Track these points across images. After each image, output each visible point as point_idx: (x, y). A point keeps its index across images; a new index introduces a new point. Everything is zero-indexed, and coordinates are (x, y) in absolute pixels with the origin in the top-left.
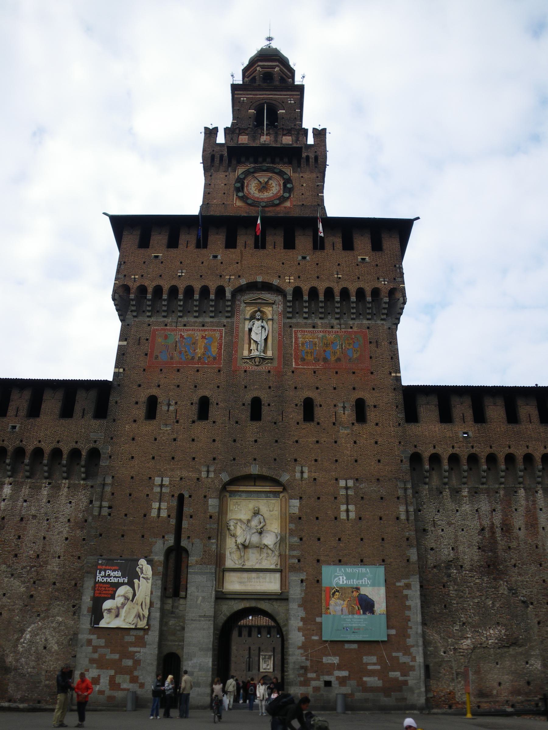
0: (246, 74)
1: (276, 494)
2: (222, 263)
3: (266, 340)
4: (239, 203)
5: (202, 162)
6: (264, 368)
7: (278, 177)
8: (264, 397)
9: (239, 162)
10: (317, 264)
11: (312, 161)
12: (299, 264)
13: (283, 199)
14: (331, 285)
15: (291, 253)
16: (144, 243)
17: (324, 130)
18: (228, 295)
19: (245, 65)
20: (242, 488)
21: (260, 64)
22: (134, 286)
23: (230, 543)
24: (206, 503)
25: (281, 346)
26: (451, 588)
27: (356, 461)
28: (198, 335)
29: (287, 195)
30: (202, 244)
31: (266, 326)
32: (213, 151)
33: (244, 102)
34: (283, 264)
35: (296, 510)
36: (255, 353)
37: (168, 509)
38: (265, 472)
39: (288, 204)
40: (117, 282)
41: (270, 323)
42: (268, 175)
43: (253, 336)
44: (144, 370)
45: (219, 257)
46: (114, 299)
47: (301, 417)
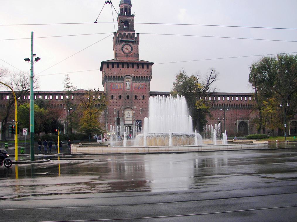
1: (131, 110)
4: (123, 53)
6: (129, 90)
8: (129, 95)
9: (122, 42)
11: (136, 42)
13: (131, 52)
15: (133, 69)
16: (108, 67)
18: (123, 78)
22: (107, 76)
23: (125, 117)
24: (122, 112)
25: (132, 87)
28: (118, 84)
29: (131, 51)
30: (118, 67)
36: (128, 88)
39: (132, 53)
43: (127, 85)
47: (135, 98)
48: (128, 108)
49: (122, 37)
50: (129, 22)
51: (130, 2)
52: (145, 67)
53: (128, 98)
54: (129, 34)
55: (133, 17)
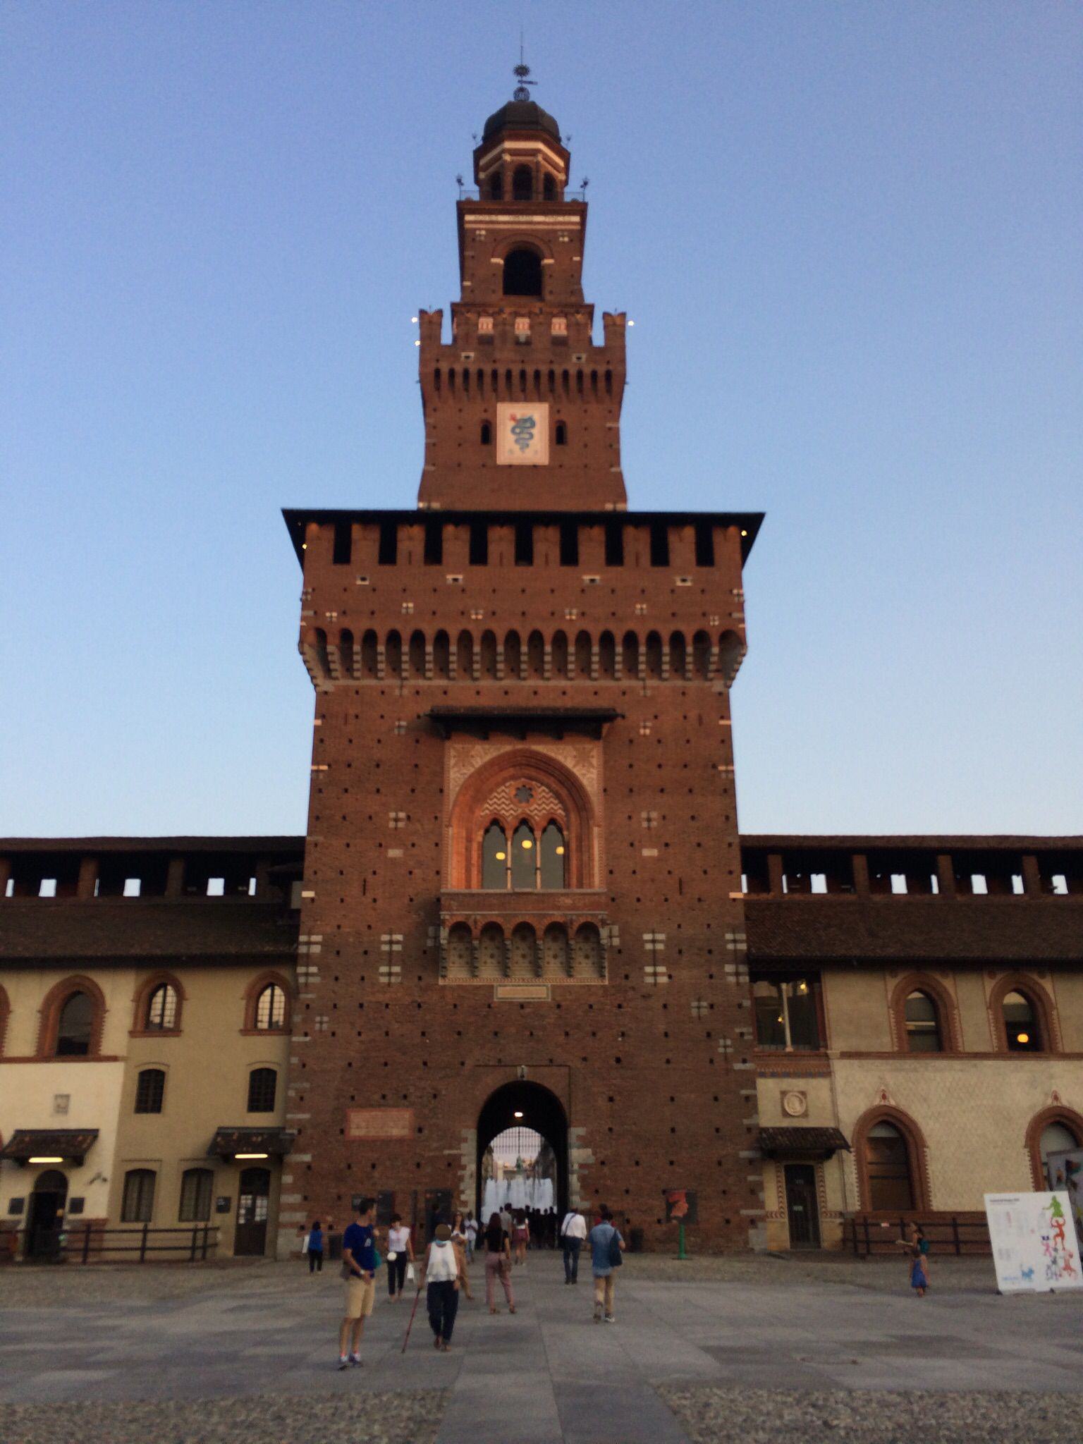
0: (482, 162)
5: (418, 379)
14: (631, 625)
16: (342, 554)
19: (480, 142)
21: (508, 145)
30: (434, 554)
33: (480, 241)
40: (304, 624)
45: (461, 582)
46: (302, 653)
50: (546, 252)
51: (559, 140)
55: (576, 219)
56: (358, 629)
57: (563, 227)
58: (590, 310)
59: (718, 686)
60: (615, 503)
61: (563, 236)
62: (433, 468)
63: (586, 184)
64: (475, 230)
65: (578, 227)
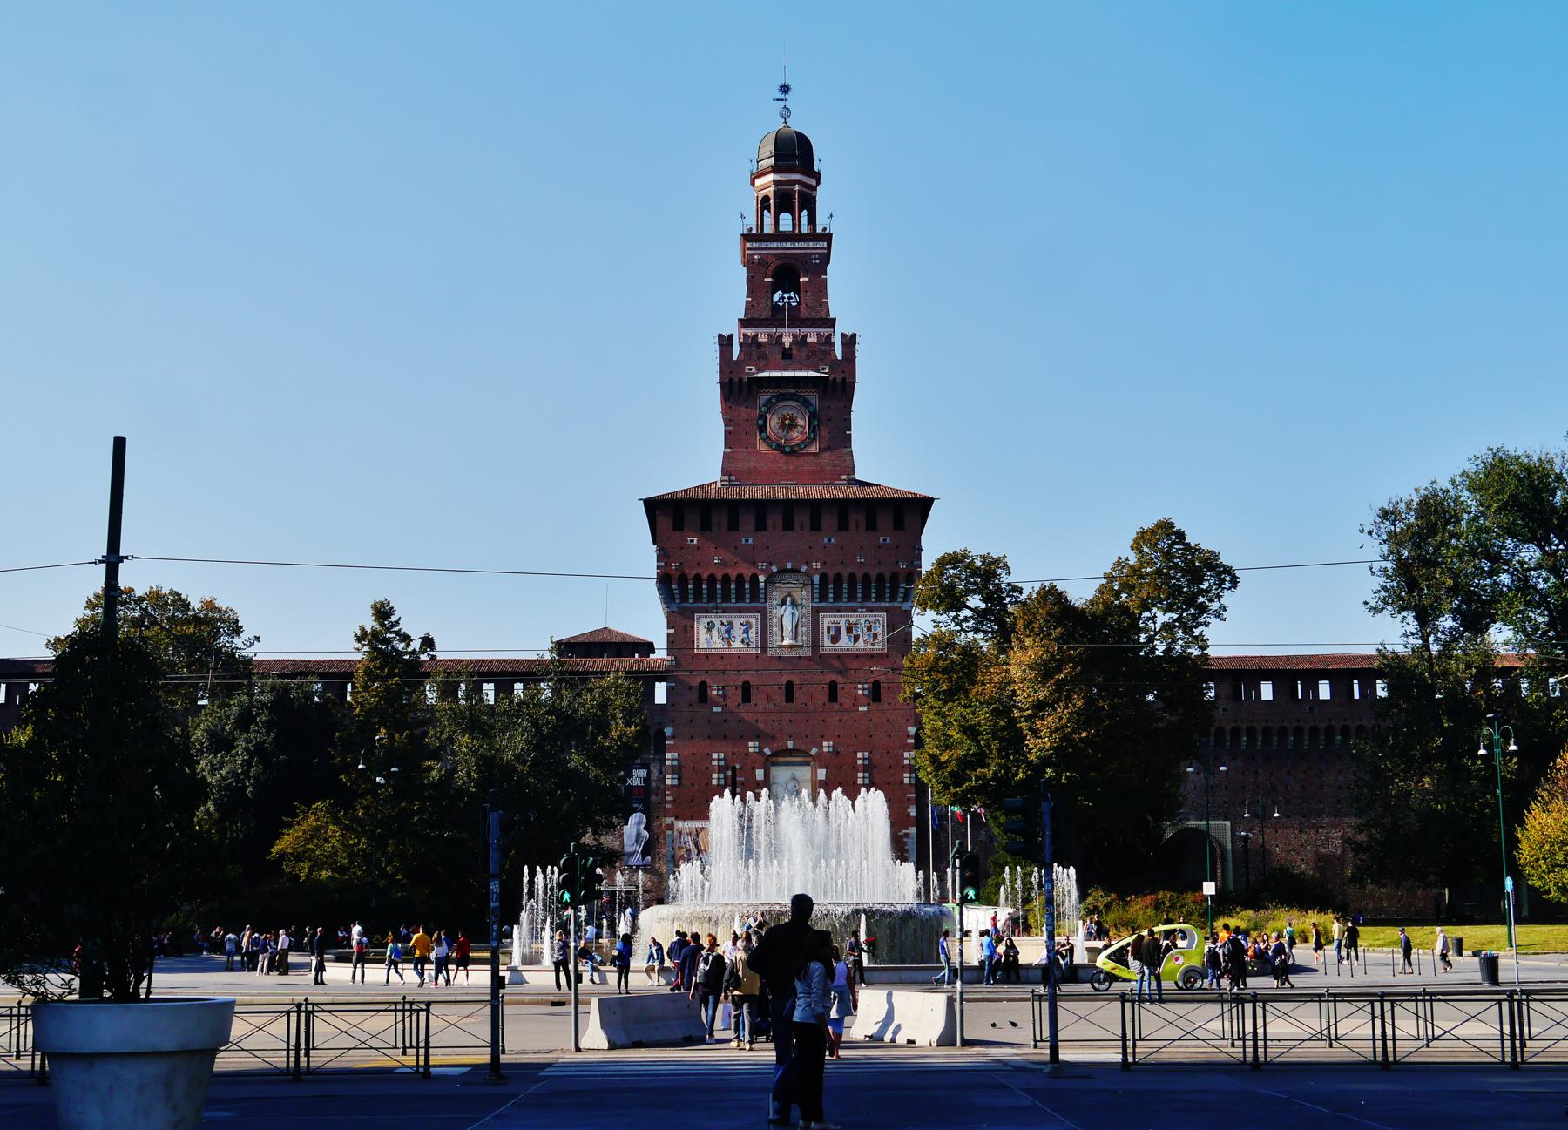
0: (758, 182)
1: (807, 764)
2: (753, 548)
3: (797, 626)
4: (763, 447)
7: (803, 409)
10: (842, 547)
12: (825, 547)
16: (678, 526)
17: (854, 335)
18: (762, 585)
20: (781, 759)
26: (942, 836)
27: (871, 736)
31: (797, 613)
32: (731, 372)
34: (810, 547)
35: (824, 778)
36: (787, 642)
37: (726, 778)
38: (798, 748)
41: (800, 608)
42: (794, 405)
44: (693, 657)
45: (750, 541)
46: (658, 589)
48: (791, 752)
49: (763, 360)
51: (814, 160)
52: (884, 520)
53: (790, 697)
54: (801, 342)
55: (825, 244)
56: (691, 573)
57: (816, 251)
58: (832, 323)
59: (906, 606)
60: (848, 475)
61: (816, 259)
62: (729, 450)
63: (831, 216)
64: (755, 254)
65: (826, 251)
